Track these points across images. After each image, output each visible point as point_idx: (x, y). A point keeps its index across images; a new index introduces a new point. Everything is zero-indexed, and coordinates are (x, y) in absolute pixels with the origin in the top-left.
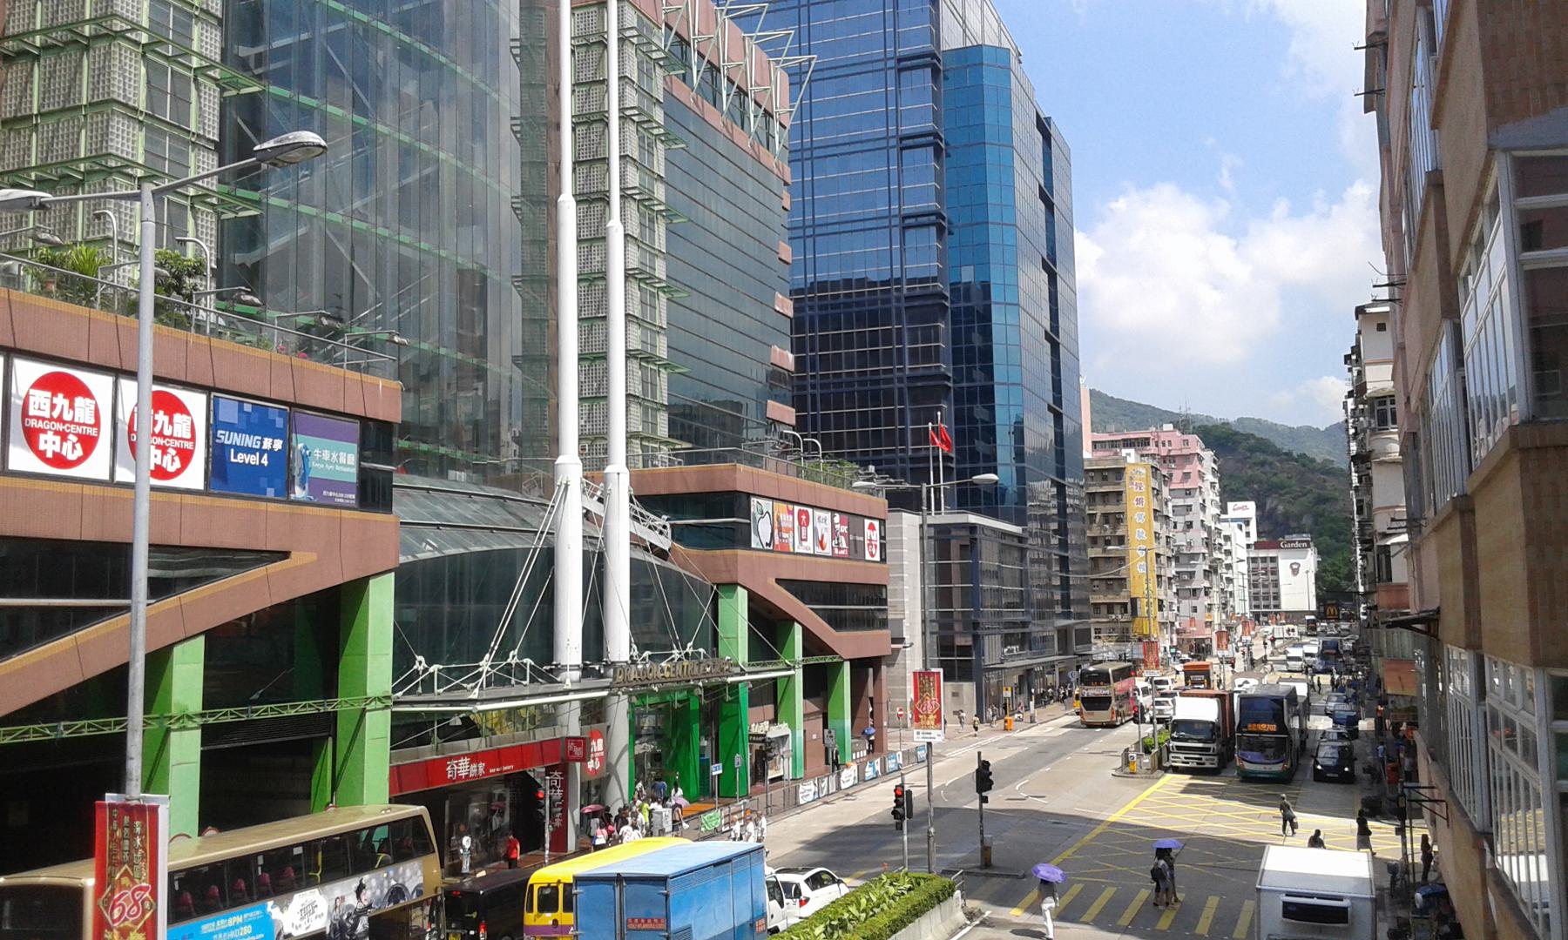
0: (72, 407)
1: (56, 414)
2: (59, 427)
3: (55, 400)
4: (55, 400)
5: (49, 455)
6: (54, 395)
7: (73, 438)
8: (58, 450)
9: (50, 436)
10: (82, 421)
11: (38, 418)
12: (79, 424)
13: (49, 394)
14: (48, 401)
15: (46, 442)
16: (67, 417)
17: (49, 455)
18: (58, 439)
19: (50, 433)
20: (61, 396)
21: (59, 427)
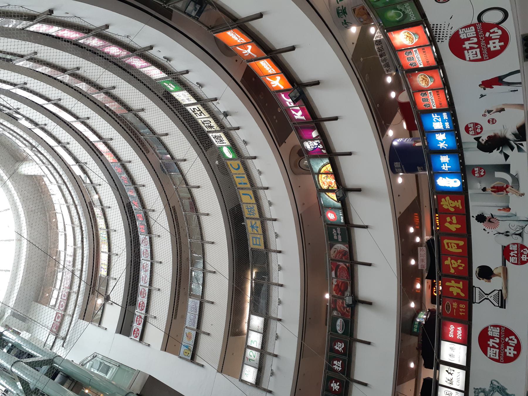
0: (468, 39)
1: (476, 46)
2: (483, 43)
3: (468, 48)
4: (468, 48)
5: (502, 44)
6: (465, 49)
7: (487, 34)
8: (498, 40)
9: (491, 46)
10: (475, 33)
11: (482, 54)
12: (477, 33)
13: (466, 52)
14: (469, 51)
15: (495, 47)
16: (475, 40)
17: (502, 44)
18: (491, 42)
19: (489, 46)
20: (464, 46)
21: (483, 43)
